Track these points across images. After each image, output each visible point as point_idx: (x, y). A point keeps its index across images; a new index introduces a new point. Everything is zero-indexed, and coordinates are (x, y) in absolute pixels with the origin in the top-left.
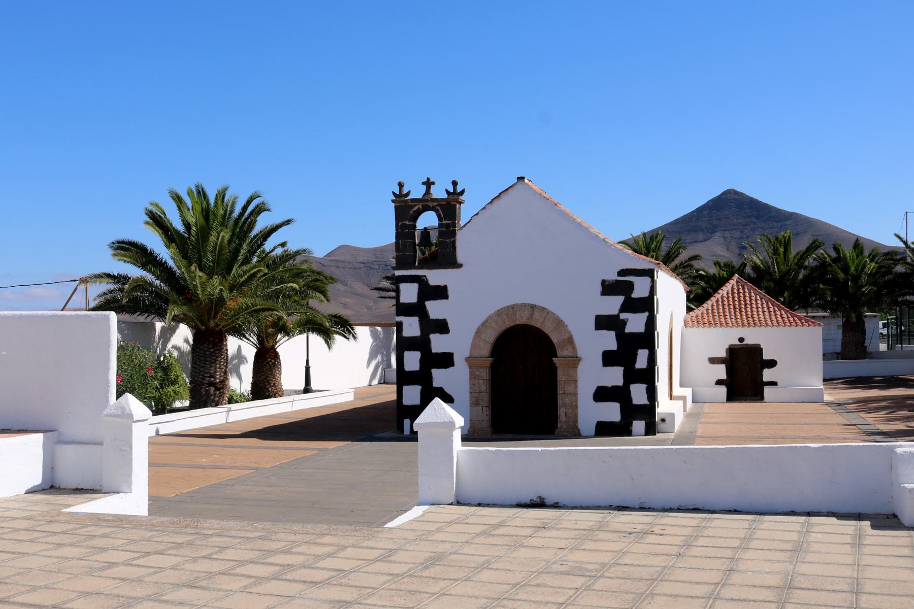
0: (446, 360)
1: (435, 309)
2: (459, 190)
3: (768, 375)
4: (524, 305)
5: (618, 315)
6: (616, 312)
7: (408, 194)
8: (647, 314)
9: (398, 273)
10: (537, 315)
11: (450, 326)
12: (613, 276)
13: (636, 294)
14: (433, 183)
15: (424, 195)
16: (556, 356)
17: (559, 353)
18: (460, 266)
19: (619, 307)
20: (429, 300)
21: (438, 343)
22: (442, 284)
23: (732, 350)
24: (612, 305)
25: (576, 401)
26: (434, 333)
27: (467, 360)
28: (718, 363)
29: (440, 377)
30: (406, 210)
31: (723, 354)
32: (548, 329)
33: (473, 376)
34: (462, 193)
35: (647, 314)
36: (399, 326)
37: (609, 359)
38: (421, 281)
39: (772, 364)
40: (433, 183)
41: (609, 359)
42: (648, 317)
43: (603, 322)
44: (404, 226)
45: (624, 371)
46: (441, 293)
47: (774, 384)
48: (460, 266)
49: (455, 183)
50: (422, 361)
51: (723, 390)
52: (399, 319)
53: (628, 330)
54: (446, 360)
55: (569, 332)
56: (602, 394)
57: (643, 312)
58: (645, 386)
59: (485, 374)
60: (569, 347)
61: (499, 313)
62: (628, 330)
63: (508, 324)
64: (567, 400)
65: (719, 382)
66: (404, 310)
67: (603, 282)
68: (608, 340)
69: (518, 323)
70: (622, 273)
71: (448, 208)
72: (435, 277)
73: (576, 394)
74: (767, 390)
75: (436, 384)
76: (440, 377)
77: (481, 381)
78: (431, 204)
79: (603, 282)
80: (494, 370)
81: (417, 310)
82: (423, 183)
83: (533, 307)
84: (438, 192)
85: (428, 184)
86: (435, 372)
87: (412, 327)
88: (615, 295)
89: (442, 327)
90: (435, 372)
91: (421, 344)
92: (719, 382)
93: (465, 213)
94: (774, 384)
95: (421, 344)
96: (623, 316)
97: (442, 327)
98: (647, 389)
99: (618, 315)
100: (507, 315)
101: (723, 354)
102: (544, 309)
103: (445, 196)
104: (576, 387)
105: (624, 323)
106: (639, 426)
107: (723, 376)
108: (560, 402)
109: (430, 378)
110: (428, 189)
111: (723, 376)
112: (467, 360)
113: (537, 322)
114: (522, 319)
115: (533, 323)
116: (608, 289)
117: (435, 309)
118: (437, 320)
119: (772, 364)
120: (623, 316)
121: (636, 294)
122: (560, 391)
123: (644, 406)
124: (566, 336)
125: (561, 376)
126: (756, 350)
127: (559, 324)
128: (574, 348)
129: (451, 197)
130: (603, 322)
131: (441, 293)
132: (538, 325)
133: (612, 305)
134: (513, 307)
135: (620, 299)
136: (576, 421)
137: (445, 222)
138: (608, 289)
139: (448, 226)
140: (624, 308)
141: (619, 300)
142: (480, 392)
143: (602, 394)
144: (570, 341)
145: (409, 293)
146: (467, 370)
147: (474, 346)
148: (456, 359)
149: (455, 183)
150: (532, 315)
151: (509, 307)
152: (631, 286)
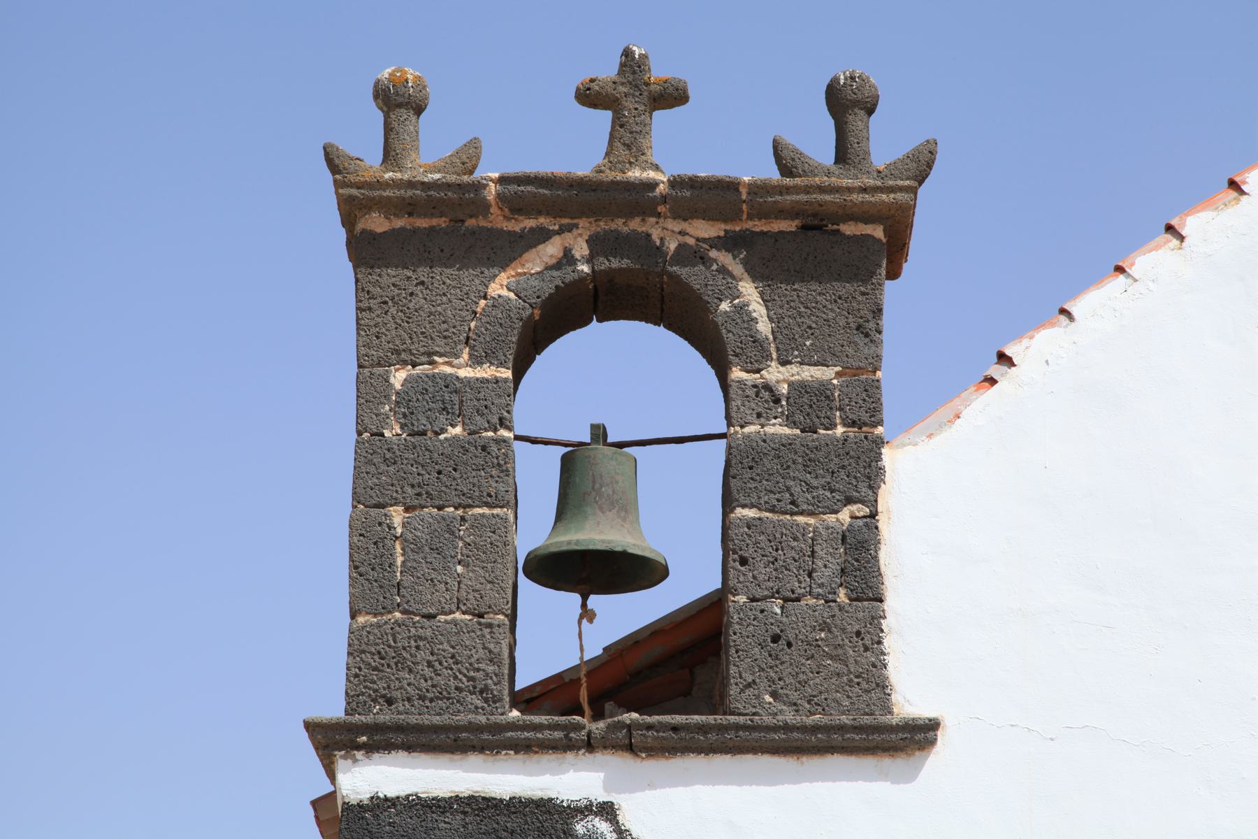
7: (470, 155)
14: (673, 96)
34: (921, 165)
48: (920, 735)
49: (847, 103)
82: (589, 96)
110: (627, 140)
139: (809, 404)
149: (847, 103)
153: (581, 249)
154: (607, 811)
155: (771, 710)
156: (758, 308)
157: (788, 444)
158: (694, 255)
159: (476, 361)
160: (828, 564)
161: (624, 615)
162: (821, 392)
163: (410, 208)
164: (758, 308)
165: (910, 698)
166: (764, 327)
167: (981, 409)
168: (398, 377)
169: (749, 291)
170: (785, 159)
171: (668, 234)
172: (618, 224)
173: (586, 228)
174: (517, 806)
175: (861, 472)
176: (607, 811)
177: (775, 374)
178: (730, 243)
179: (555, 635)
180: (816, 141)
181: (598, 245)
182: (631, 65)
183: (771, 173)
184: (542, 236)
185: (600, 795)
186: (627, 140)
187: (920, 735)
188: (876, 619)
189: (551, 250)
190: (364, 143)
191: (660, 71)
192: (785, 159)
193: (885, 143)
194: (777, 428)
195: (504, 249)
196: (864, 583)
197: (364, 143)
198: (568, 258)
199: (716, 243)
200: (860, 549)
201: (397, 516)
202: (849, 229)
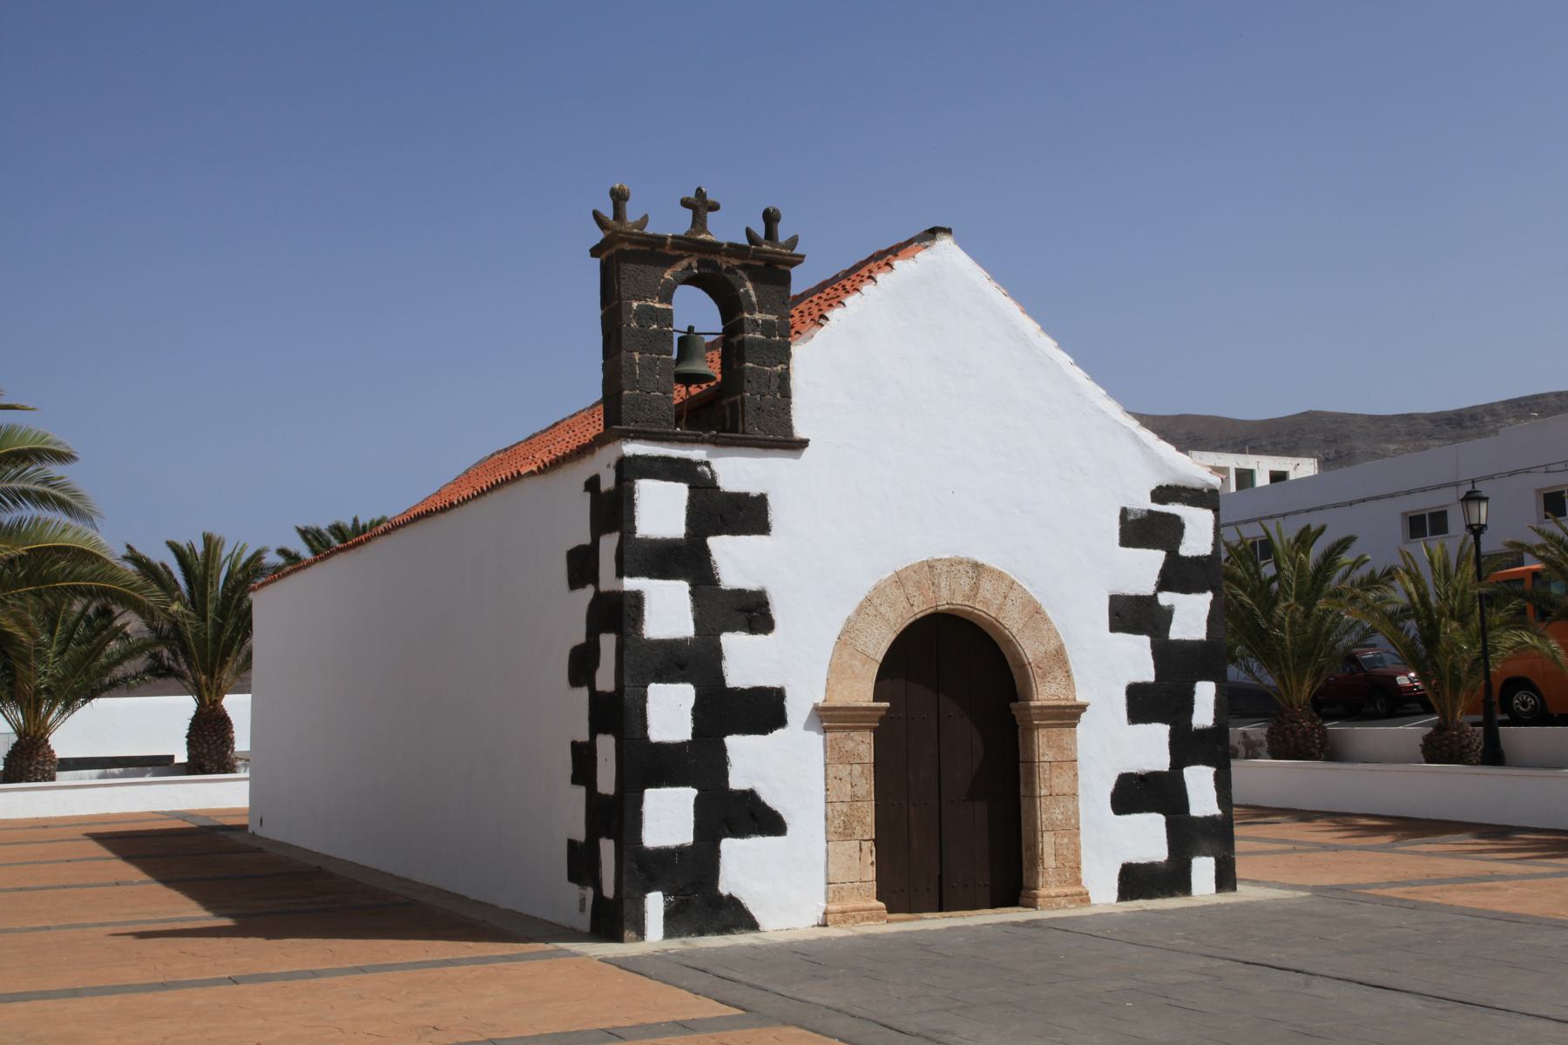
0: (764, 710)
1: (736, 561)
8: (1209, 596)
10: (987, 586)
11: (777, 611)
12: (1143, 502)
14: (714, 207)
20: (718, 532)
21: (745, 661)
22: (755, 491)
25: (1076, 814)
26: (733, 630)
29: (749, 761)
32: (1012, 623)
33: (834, 757)
35: (1209, 596)
37: (1143, 704)
40: (714, 207)
41: (1143, 704)
42: (1212, 603)
45: (1172, 735)
46: (749, 515)
48: (803, 444)
49: (771, 218)
50: (700, 712)
53: (1177, 632)
54: (764, 710)
56: (1133, 794)
57: (1202, 590)
59: (863, 745)
60: (1059, 674)
61: (899, 580)
62: (1177, 632)
63: (921, 607)
64: (1058, 814)
69: (943, 607)
72: (736, 471)
75: (737, 782)
76: (749, 761)
79: (1124, 512)
81: (684, 559)
82: (685, 203)
83: (976, 566)
85: (700, 206)
86: (733, 743)
89: (753, 612)
90: (733, 743)
91: (694, 661)
96: (1165, 599)
97: (753, 612)
98: (1217, 777)
100: (918, 585)
102: (1001, 576)
105: (1167, 614)
106: (1203, 869)
109: (720, 762)
110: (699, 222)
114: (950, 596)
117: (736, 561)
118: (740, 593)
120: (1165, 599)
123: (1209, 821)
124: (1051, 647)
125: (1044, 744)
127: (1035, 612)
131: (749, 515)
133: (1141, 570)
134: (930, 566)
142: (855, 799)
143: (1133, 794)
144: (1059, 657)
147: (837, 670)
148: (798, 708)
149: (771, 218)
150: (976, 587)
153: (695, 264)
154: (707, 464)
155: (759, 434)
156: (752, 292)
157: (762, 341)
158: (730, 270)
159: (661, 302)
160: (775, 383)
162: (772, 323)
163: (639, 243)
164: (752, 292)
165: (800, 432)
166: (754, 299)
167: (820, 335)
169: (749, 285)
170: (749, 233)
171: (724, 262)
174: (679, 461)
175: (784, 355)
176: (707, 464)
177: (757, 316)
178: (744, 267)
180: (760, 231)
181: (701, 263)
183: (744, 241)
184: (681, 258)
185: (705, 459)
186: (699, 222)
187: (803, 444)
188: (789, 404)
189: (685, 263)
190: (608, 212)
191: (710, 197)
192: (749, 233)
193: (783, 234)
194: (758, 336)
195: (669, 262)
196: (786, 393)
197: (608, 212)
198: (690, 267)
200: (785, 378)
201: (637, 356)
202: (781, 267)
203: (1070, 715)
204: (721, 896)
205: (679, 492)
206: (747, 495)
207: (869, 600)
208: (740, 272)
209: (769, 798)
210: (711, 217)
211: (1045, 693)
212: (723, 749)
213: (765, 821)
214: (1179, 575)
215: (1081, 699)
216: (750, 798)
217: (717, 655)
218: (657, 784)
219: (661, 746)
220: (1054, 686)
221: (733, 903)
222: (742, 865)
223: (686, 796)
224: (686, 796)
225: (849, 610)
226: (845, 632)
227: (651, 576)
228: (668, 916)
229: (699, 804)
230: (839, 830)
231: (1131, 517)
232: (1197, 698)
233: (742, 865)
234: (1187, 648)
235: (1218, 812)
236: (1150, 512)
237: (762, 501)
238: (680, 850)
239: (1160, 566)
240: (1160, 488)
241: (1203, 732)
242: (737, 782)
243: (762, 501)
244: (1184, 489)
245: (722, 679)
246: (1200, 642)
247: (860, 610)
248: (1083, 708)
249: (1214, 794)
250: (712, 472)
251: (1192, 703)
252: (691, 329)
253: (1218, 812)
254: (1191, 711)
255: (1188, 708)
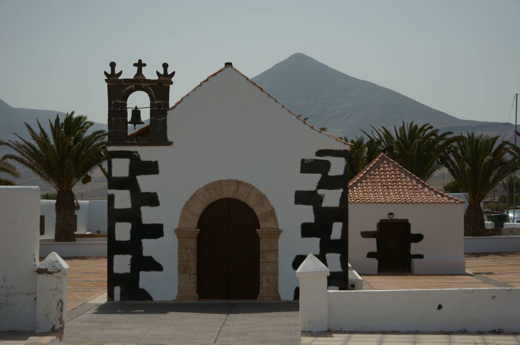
0: (156, 231)
1: (146, 183)
2: (169, 72)
3: (415, 248)
4: (231, 181)
5: (316, 191)
6: (313, 188)
8: (341, 190)
9: (110, 149)
11: (160, 199)
12: (311, 156)
13: (331, 173)
14: (145, 65)
15: (136, 76)
16: (259, 228)
17: (262, 225)
18: (171, 143)
19: (316, 184)
21: (149, 215)
22: (153, 160)
23: (382, 224)
24: (310, 182)
25: (277, 268)
26: (145, 205)
27: (176, 231)
28: (369, 237)
29: (149, 247)
30: (118, 89)
31: (374, 228)
32: (252, 202)
33: (181, 246)
35: (341, 190)
36: (111, 199)
38: (133, 157)
39: (419, 238)
40: (145, 65)
41: (307, 230)
42: (343, 193)
43: (302, 198)
44: (117, 105)
45: (321, 242)
46: (152, 168)
47: (420, 256)
48: (171, 143)
49: (165, 66)
51: (374, 262)
52: (111, 192)
53: (324, 204)
54: (156, 231)
55: (272, 206)
57: (338, 188)
58: (339, 255)
59: (193, 244)
61: (207, 188)
62: (324, 204)
63: (215, 197)
65: (370, 255)
66: (116, 183)
67: (303, 161)
68: (307, 213)
69: (224, 196)
70: (320, 153)
71: (159, 88)
72: (147, 153)
73: (276, 263)
74: (415, 261)
75: (145, 253)
76: (149, 247)
77: (189, 251)
78: (143, 85)
79: (303, 161)
80: (200, 239)
81: (128, 184)
82: (135, 65)
83: (238, 183)
84: (150, 74)
85: (140, 65)
86: (144, 241)
87: (123, 199)
88: (314, 173)
89: (152, 200)
90: (144, 241)
91: (132, 216)
92: (370, 255)
93: (176, 94)
94: (420, 256)
95: (132, 216)
96: (320, 192)
97: (152, 200)
98: (341, 258)
99: (316, 191)
101: (374, 228)
102: (248, 185)
103: (156, 78)
104: (277, 256)
105: (321, 198)
107: (374, 249)
108: (262, 269)
111: (374, 249)
112: (176, 231)
113: (242, 196)
114: (228, 193)
115: (238, 197)
116: (307, 167)
117: (146, 183)
119: (419, 238)
120: (320, 192)
121: (331, 173)
122: (262, 260)
125: (263, 246)
126: (405, 224)
127: (262, 198)
128: (276, 221)
129: (162, 78)
130: (302, 198)
131: (152, 168)
132: (243, 199)
133: (310, 182)
134: (220, 182)
135: (317, 177)
136: (276, 287)
137: (156, 102)
138: (307, 167)
139: (159, 105)
140: (321, 185)
141: (317, 177)
144: (272, 214)
145: (121, 168)
146: (176, 240)
147: (183, 218)
149: (165, 66)
150: (237, 190)
151: (216, 182)
152: (327, 165)
154: (137, 152)
161: (139, 127)
165: (170, 138)
168: (113, 102)
172: (137, 84)
173: (134, 84)
178: (150, 86)
179: (131, 129)
182: (140, 61)
184: (129, 85)
185: (136, 150)
189: (130, 87)
191: (143, 62)
194: (155, 108)
196: (165, 127)
199: (149, 86)
200: (165, 121)
202: (164, 85)
203: (276, 233)
204: (140, 289)
205: (126, 162)
206: (151, 161)
207: (195, 195)
208: (149, 88)
209: (158, 259)
210: (143, 68)
211: (265, 225)
212: (141, 243)
213: (153, 265)
214: (328, 182)
215: (280, 227)
216: (150, 259)
217: (139, 214)
218: (119, 253)
219: (120, 242)
220: (269, 224)
221: (144, 291)
222: (146, 280)
223: (129, 257)
224: (129, 257)
225: (187, 198)
226: (185, 206)
227: (117, 189)
228: (122, 294)
229: (132, 260)
230: (183, 269)
231: (306, 162)
232: (333, 228)
233: (146, 280)
234: (330, 210)
235: (342, 270)
236: (315, 160)
237: (156, 163)
238: (126, 274)
239: (319, 180)
240: (320, 151)
241: (336, 241)
242: (145, 253)
243: (156, 163)
244: (332, 150)
245: (141, 221)
246: (336, 208)
247: (192, 198)
248: (280, 231)
249: (339, 264)
250: (138, 155)
251: (331, 230)
252: (136, 107)
253: (342, 270)
254: (331, 233)
255: (329, 231)
